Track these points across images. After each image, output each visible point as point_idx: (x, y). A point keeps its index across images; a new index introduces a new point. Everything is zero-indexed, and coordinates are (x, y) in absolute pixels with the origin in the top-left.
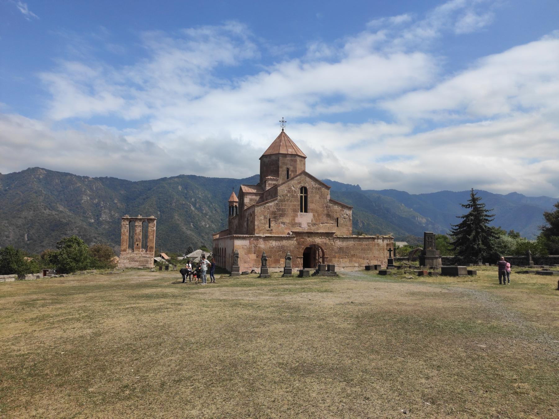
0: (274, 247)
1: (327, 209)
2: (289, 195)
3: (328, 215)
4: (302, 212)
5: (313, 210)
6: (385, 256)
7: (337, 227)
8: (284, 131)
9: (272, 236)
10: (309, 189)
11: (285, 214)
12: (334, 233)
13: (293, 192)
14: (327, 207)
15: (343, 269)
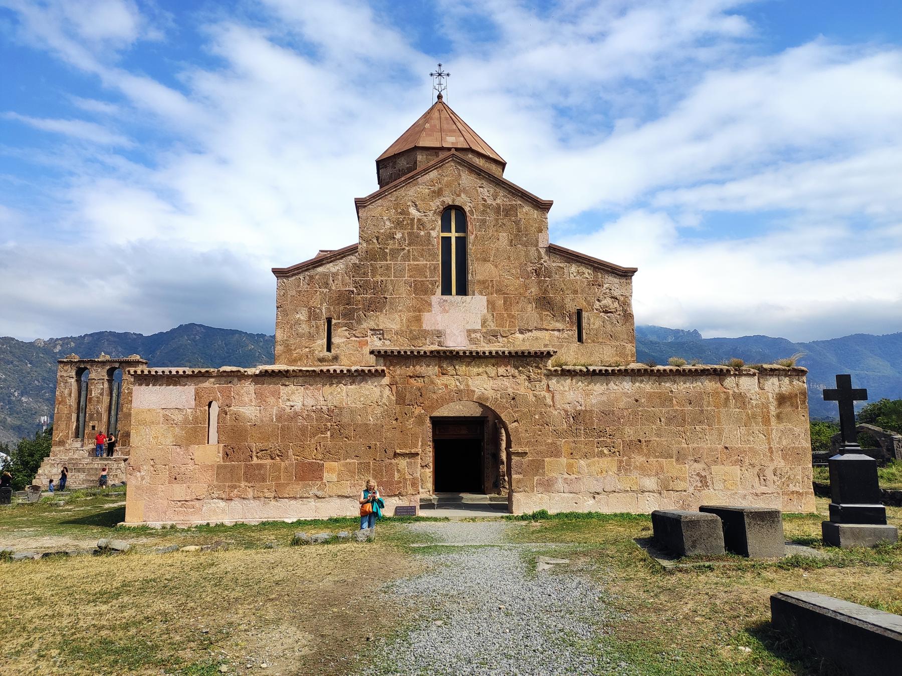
0: (296, 414)
1: (539, 282)
2: (398, 236)
3: (545, 303)
4: (451, 295)
5: (486, 286)
6: (775, 445)
7: (578, 343)
8: (444, 100)
9: (288, 371)
10: (471, 212)
11: (385, 303)
12: (548, 353)
13: (412, 225)
14: (537, 273)
15: (591, 501)
